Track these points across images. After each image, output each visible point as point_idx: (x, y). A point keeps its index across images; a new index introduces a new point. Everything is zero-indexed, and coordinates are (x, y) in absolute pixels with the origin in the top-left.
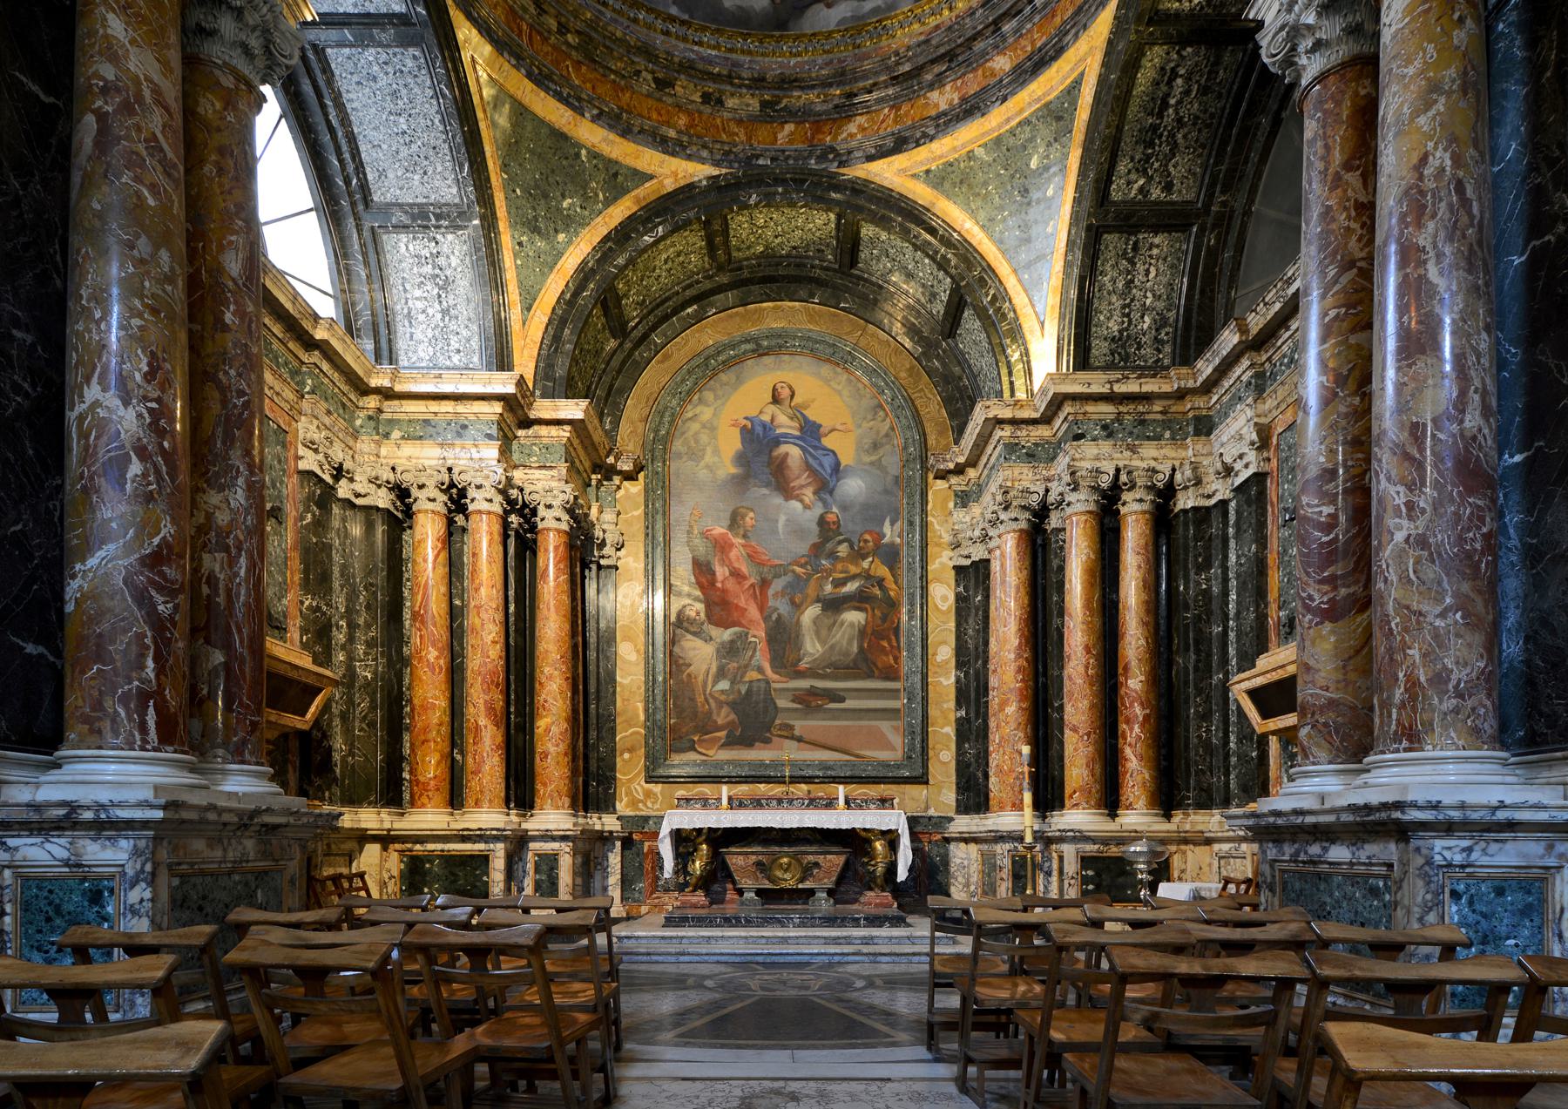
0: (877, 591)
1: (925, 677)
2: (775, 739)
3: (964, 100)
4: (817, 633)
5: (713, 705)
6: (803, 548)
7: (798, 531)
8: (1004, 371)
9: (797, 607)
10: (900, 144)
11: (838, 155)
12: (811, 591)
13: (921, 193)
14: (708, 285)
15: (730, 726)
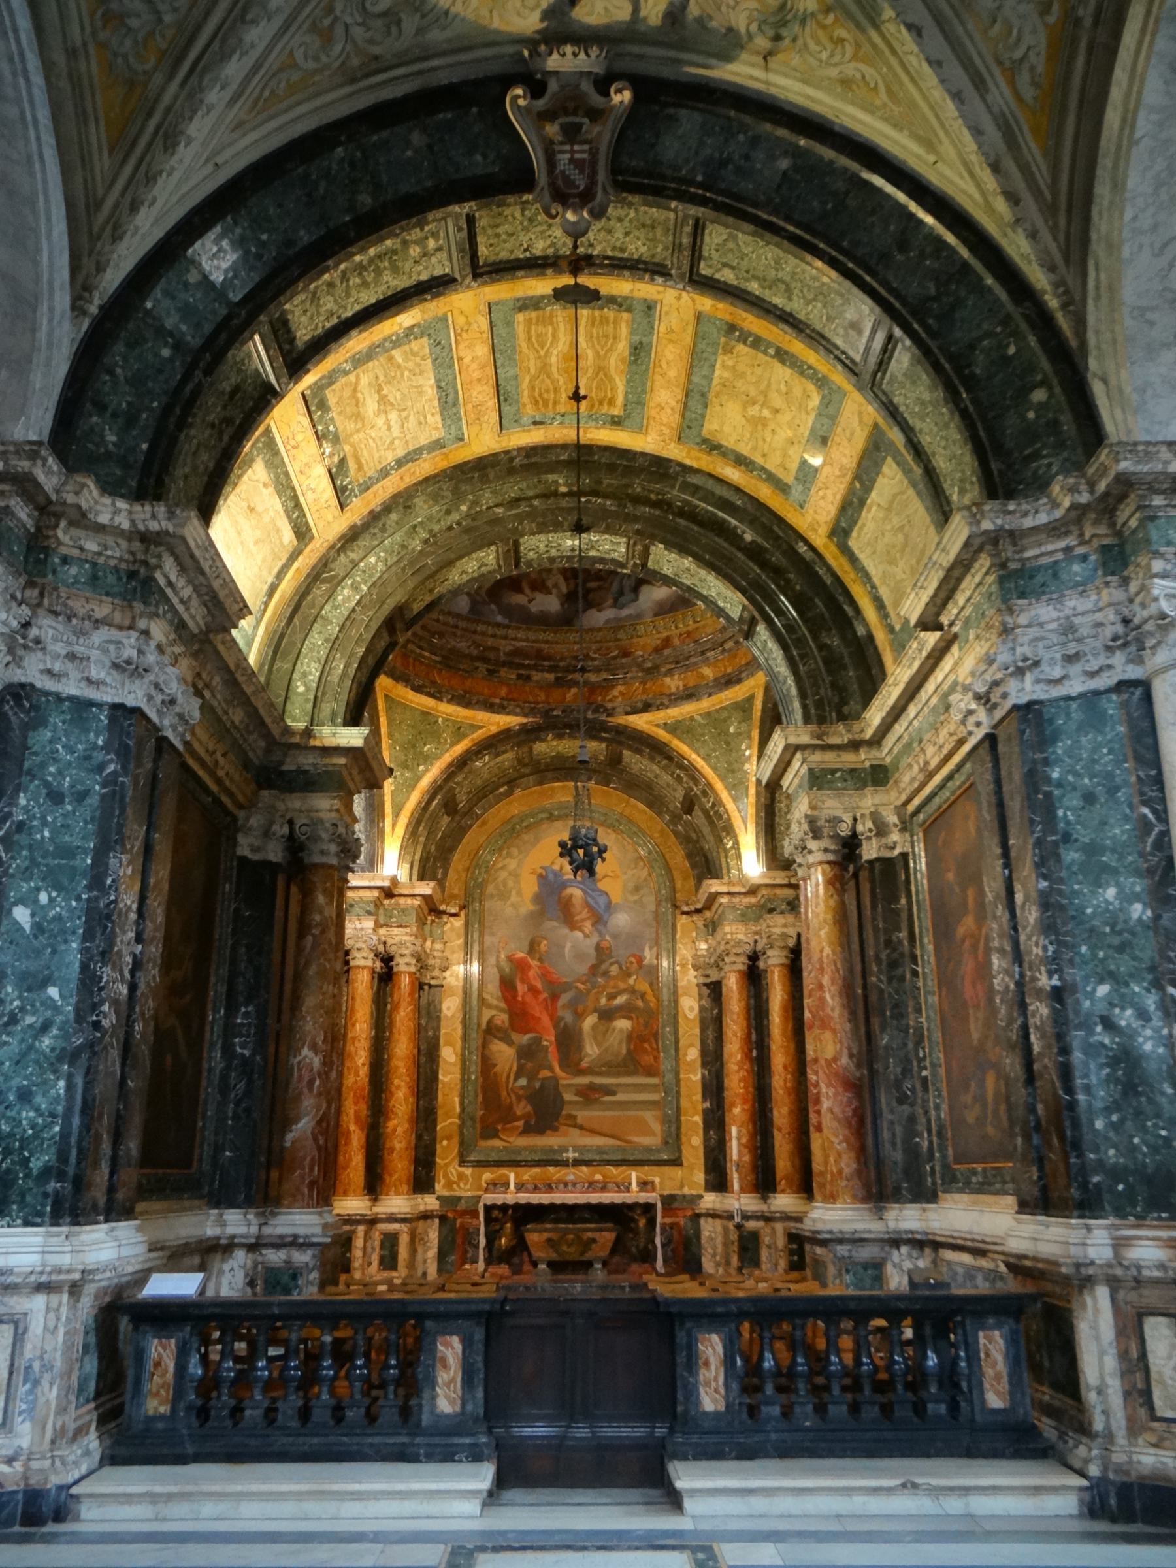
0: (640, 1003)
1: (677, 1074)
2: (562, 1128)
3: (686, 688)
4: (595, 1038)
5: (513, 1097)
6: (583, 969)
7: (579, 956)
8: (722, 855)
9: (580, 1016)
10: (646, 708)
11: (606, 710)
12: (590, 1004)
13: (662, 735)
14: (516, 775)
15: (527, 1116)
